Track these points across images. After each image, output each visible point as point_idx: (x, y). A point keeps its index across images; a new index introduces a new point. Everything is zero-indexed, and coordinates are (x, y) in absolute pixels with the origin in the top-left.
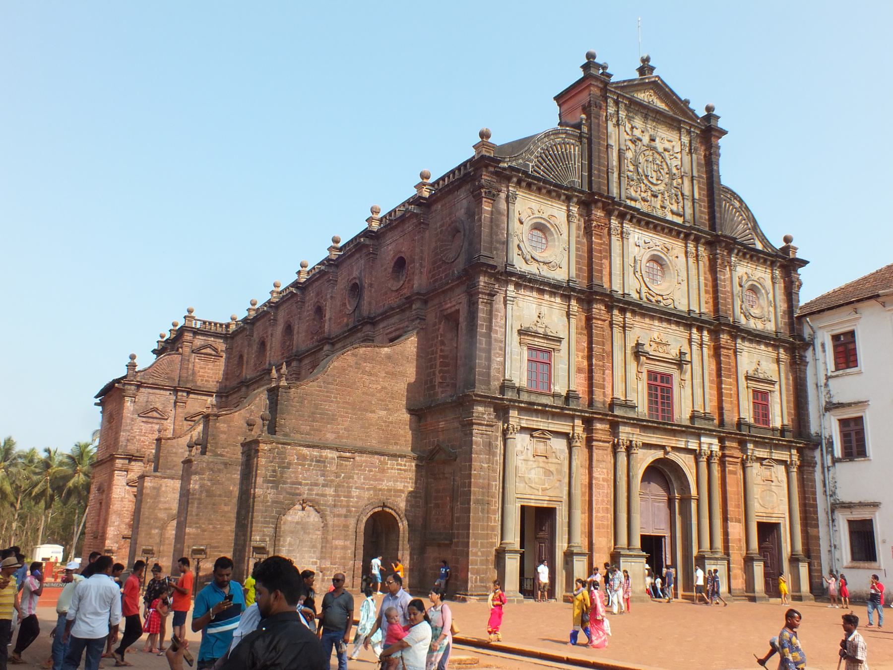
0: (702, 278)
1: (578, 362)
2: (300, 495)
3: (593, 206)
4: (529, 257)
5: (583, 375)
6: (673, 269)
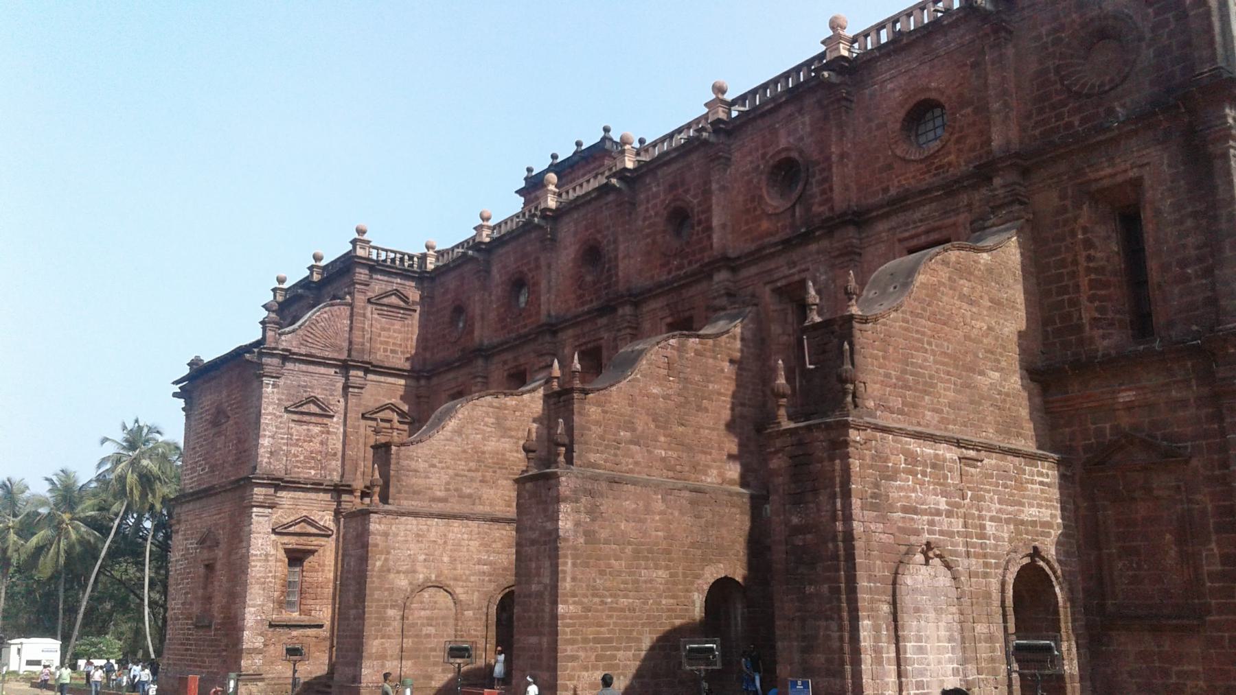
2: (917, 532)
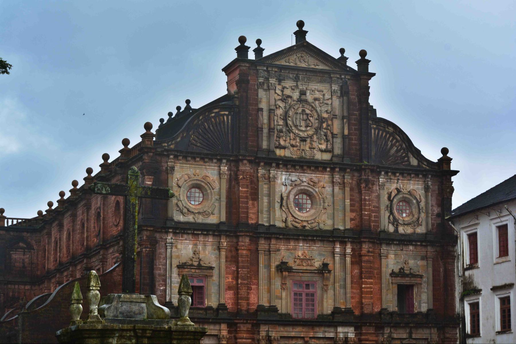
0: (348, 202)
1: (229, 282)
3: (240, 164)
4: (185, 210)
5: (232, 292)
6: (319, 198)
